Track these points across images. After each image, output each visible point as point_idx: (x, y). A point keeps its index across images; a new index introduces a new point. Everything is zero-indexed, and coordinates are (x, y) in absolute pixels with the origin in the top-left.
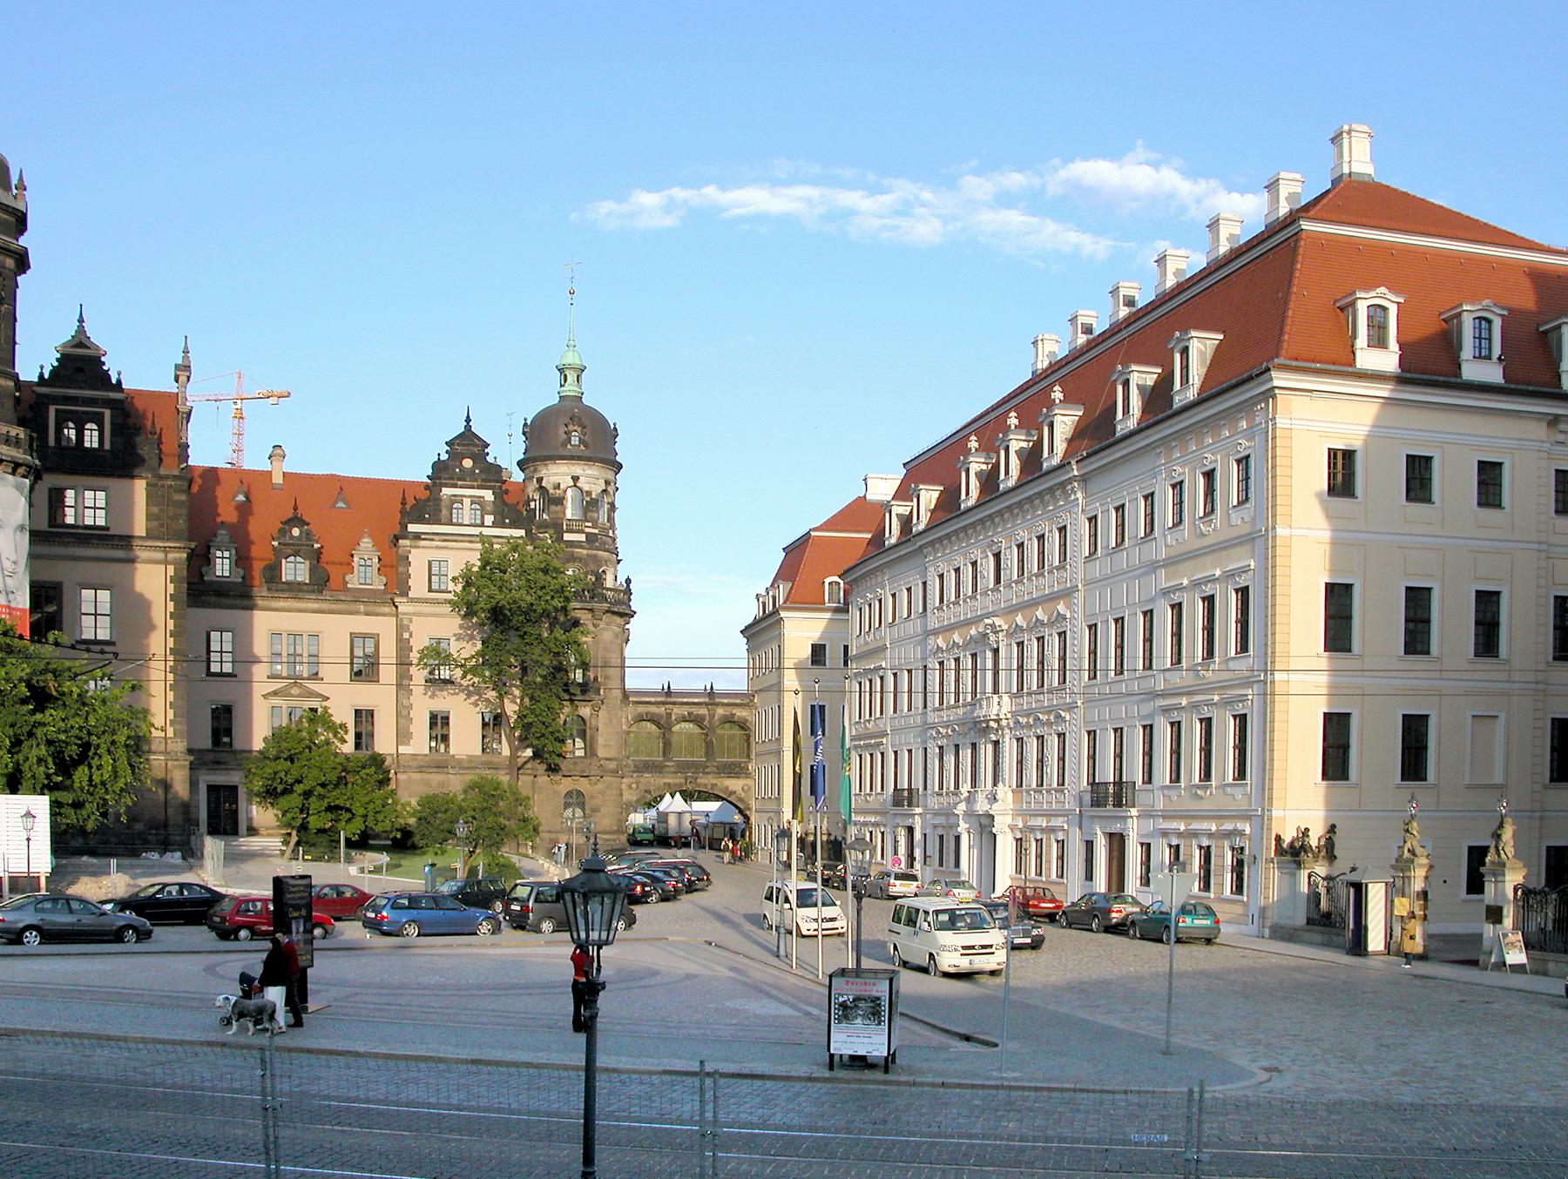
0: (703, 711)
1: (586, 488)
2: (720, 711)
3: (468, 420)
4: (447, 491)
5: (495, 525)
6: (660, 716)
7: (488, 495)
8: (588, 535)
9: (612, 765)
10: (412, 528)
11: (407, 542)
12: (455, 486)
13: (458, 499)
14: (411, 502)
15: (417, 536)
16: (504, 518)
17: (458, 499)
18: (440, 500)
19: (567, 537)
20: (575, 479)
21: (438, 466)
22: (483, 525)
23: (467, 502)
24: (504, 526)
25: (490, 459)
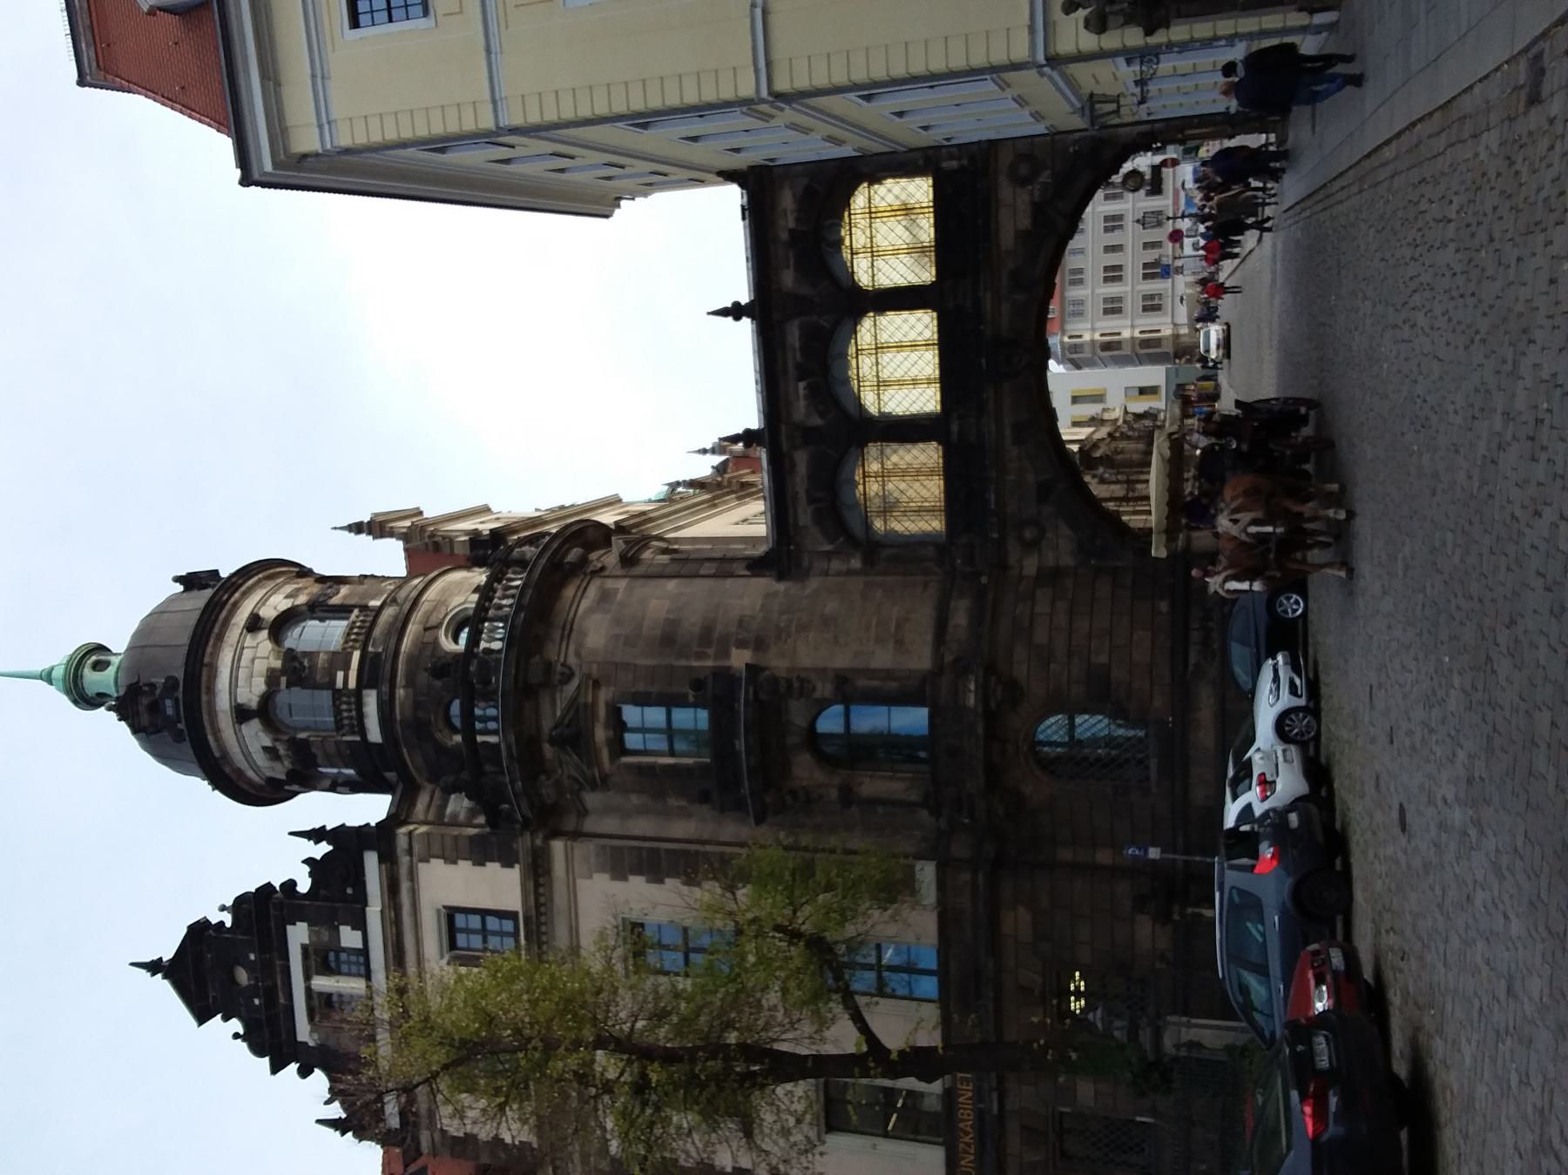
0: (793, 334)
1: (260, 686)
2: (788, 279)
3: (154, 967)
4: (304, 1031)
5: (360, 924)
7: (298, 934)
13: (322, 1005)
14: (336, 1111)
16: (345, 898)
19: (375, 735)
20: (242, 714)
22: (365, 952)
23: (321, 983)
24: (362, 899)
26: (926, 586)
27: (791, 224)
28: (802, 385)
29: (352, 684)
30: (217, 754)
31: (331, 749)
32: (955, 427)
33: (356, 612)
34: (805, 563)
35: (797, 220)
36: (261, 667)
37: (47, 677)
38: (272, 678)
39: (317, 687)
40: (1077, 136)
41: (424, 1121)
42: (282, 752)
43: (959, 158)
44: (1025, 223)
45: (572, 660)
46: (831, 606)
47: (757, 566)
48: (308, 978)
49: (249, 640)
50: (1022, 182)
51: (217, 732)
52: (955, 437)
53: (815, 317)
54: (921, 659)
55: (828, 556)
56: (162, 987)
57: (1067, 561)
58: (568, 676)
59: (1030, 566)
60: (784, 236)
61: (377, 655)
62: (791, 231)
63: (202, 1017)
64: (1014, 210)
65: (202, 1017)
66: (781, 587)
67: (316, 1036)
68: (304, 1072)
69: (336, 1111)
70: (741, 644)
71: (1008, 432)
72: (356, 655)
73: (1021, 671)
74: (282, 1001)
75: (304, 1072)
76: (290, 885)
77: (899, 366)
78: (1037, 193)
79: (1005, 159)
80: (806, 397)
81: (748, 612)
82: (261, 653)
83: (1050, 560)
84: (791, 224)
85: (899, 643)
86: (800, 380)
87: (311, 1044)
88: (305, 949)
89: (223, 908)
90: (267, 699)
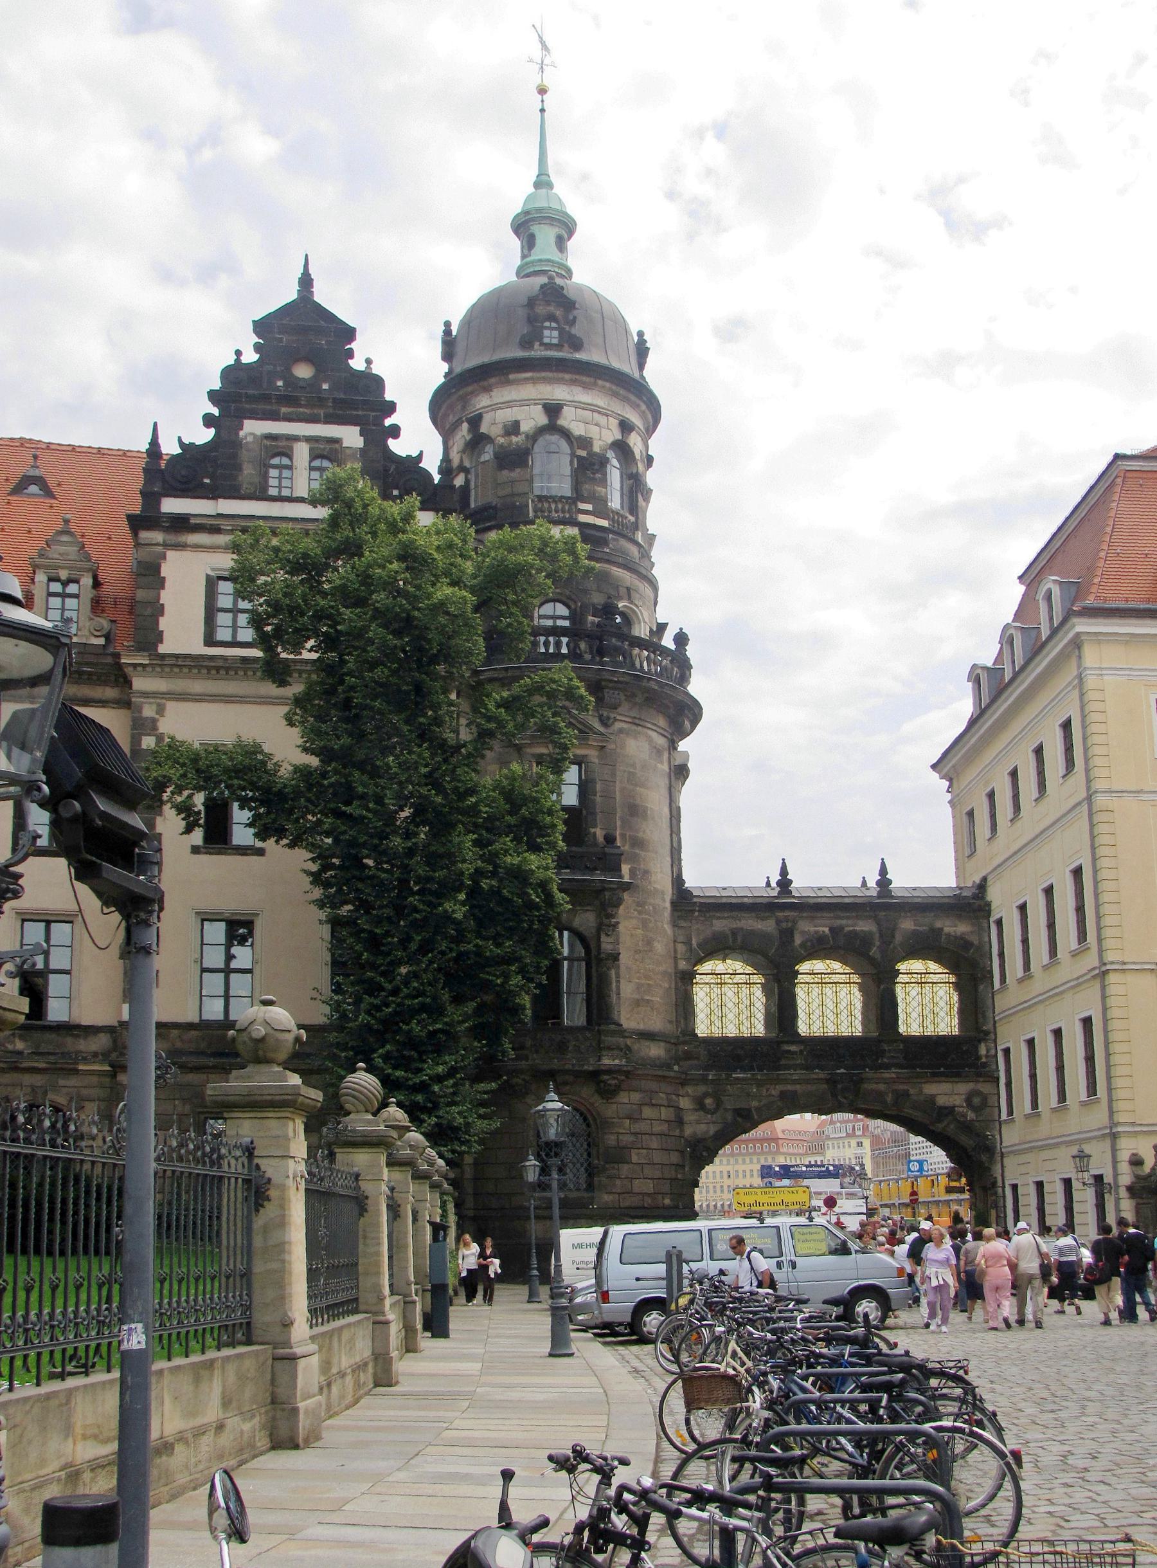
0: (865, 926)
1: (578, 429)
2: (907, 925)
3: (306, 281)
4: (253, 428)
6: (764, 936)
7: (351, 437)
8: (583, 526)
9: (656, 1051)
10: (171, 505)
11: (158, 536)
12: (274, 417)
13: (280, 447)
14: (170, 448)
15: (181, 523)
17: (280, 447)
18: (237, 444)
20: (553, 410)
21: (234, 374)
23: (302, 452)
25: (358, 364)
26: (671, 1022)
27: (946, 930)
28: (826, 930)
29: (583, 518)
30: (511, 377)
31: (521, 488)
32: (793, 1048)
33: (632, 519)
34: (683, 923)
35: (948, 935)
36: (593, 432)
37: (542, 182)
38: (585, 442)
39: (576, 485)
40: (998, 1137)
41: (172, 538)
42: (514, 439)
43: (987, 1056)
44: (941, 1101)
45: (618, 725)
46: (659, 947)
47: (678, 881)
48: (308, 439)
49: (614, 423)
50: (968, 1100)
51: (534, 381)
52: (786, 1047)
53: (878, 943)
54: (628, 1019)
55: (688, 943)
56: (290, 294)
57: (688, 1131)
58: (605, 722)
59: (685, 1103)
60: (938, 924)
61: (605, 543)
62: (942, 929)
63: (261, 327)
64: (949, 1093)
65: (261, 327)
66: (668, 905)
67: (250, 439)
68: (208, 420)
69: (170, 448)
70: (632, 872)
71: (790, 1087)
72: (604, 523)
73: (623, 1097)
74: (284, 410)
75: (208, 420)
76: (395, 432)
77: (830, 1004)
78: (961, 1110)
79: (985, 1088)
80: (817, 932)
81: (653, 878)
82: (604, 435)
83: (689, 1117)
84: (946, 930)
85: (637, 1003)
86: (831, 929)
87: (241, 433)
88: (337, 441)
89: (369, 362)
90: (566, 434)
